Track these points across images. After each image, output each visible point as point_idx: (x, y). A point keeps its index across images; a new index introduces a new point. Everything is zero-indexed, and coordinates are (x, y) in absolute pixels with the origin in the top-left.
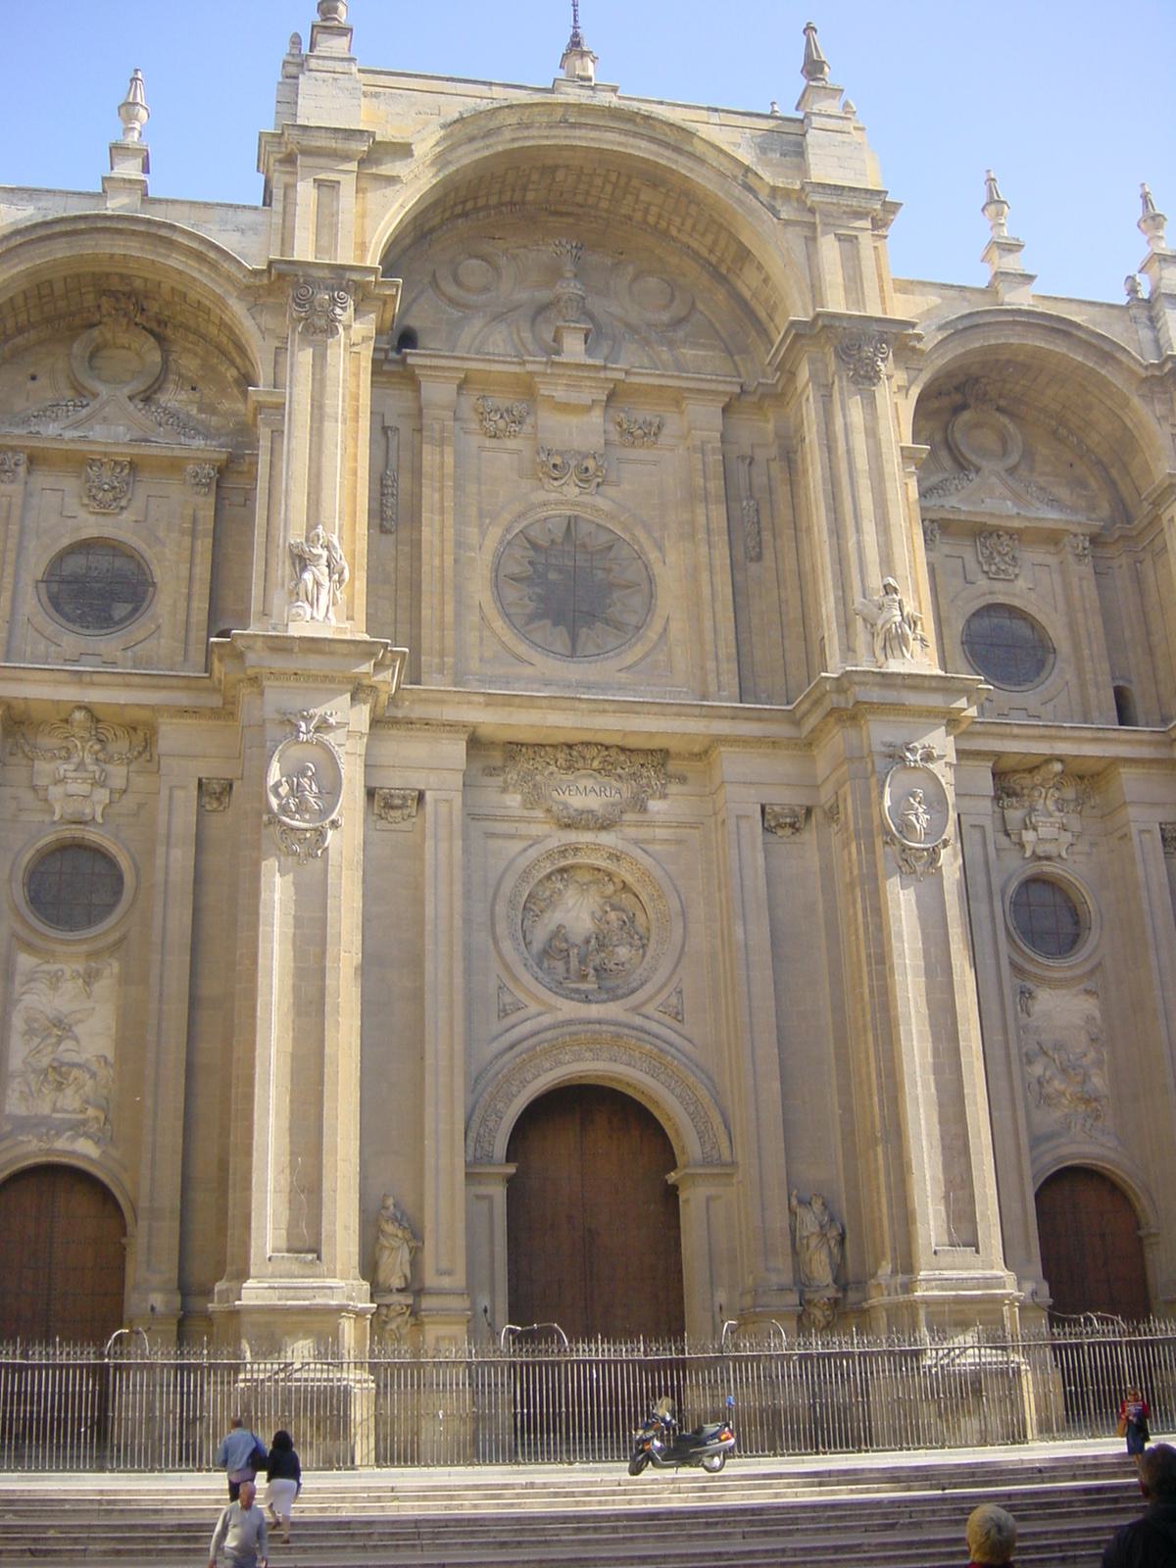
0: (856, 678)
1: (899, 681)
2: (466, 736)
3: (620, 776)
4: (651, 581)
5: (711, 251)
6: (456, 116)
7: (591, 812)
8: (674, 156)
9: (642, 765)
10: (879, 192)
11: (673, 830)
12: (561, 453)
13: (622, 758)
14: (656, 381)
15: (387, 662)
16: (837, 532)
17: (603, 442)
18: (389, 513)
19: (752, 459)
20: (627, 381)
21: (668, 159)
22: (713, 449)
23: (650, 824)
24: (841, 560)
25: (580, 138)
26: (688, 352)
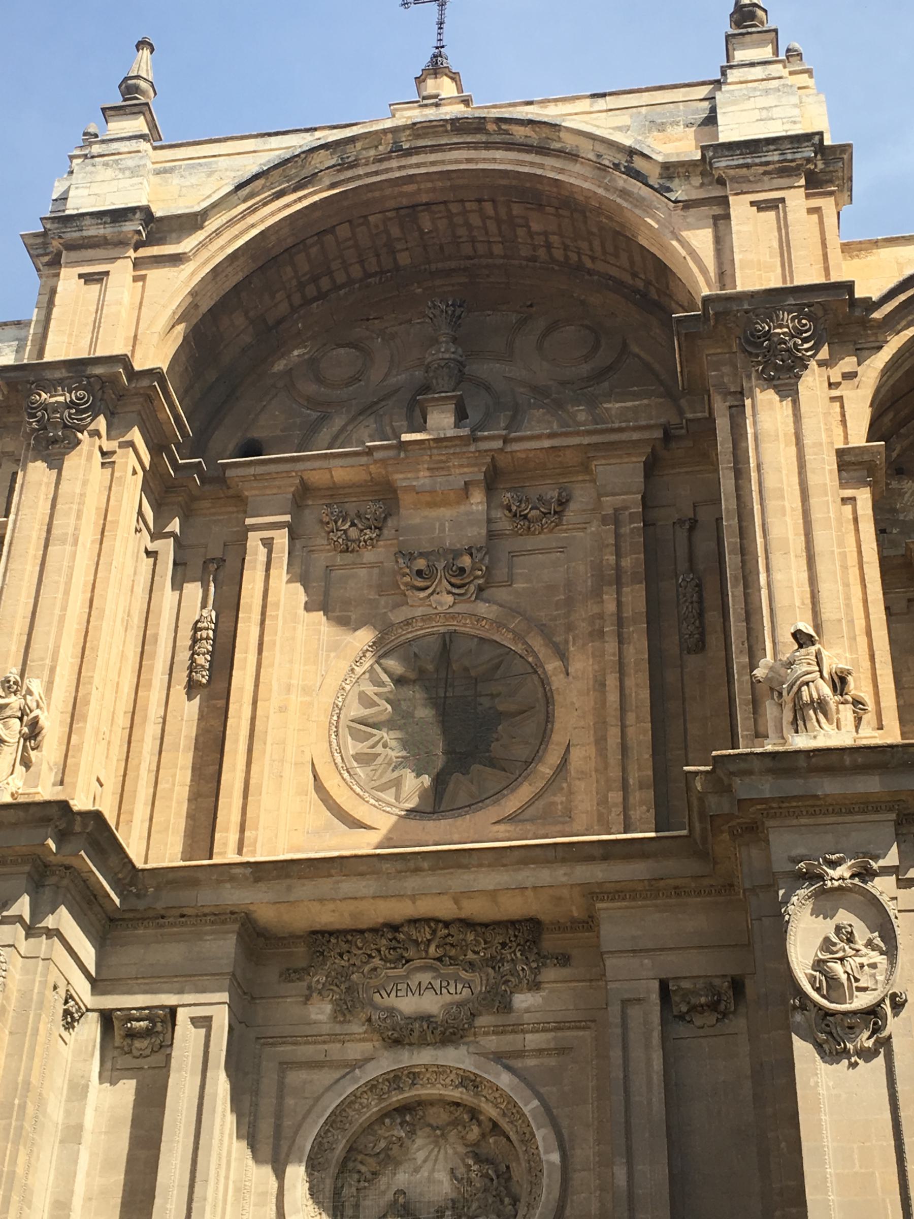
0: (732, 768)
1: (802, 762)
2: (236, 927)
3: (471, 964)
4: (548, 700)
5: (634, 275)
6: (255, 169)
7: (427, 1018)
8: (537, 159)
9: (504, 945)
10: (808, 137)
11: (550, 1035)
12: (421, 555)
13: (471, 937)
14: (547, 443)
15: (78, 828)
16: (745, 578)
17: (484, 532)
18: (200, 660)
19: (693, 524)
20: (508, 449)
21: (532, 164)
22: (630, 513)
23: (517, 1028)
24: (751, 614)
25: (418, 165)
26: (614, 406)
